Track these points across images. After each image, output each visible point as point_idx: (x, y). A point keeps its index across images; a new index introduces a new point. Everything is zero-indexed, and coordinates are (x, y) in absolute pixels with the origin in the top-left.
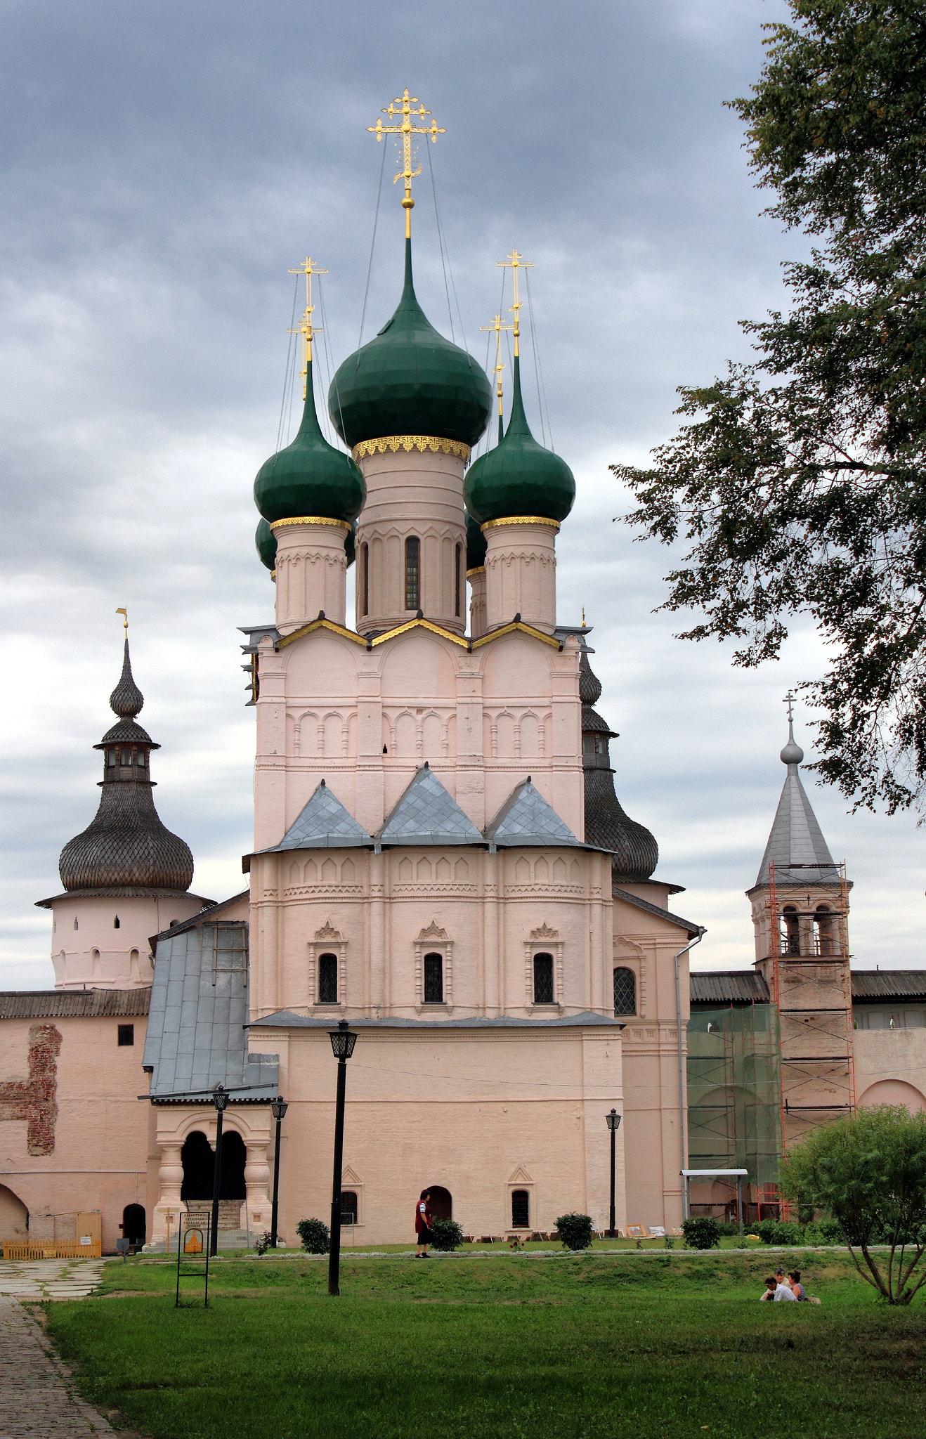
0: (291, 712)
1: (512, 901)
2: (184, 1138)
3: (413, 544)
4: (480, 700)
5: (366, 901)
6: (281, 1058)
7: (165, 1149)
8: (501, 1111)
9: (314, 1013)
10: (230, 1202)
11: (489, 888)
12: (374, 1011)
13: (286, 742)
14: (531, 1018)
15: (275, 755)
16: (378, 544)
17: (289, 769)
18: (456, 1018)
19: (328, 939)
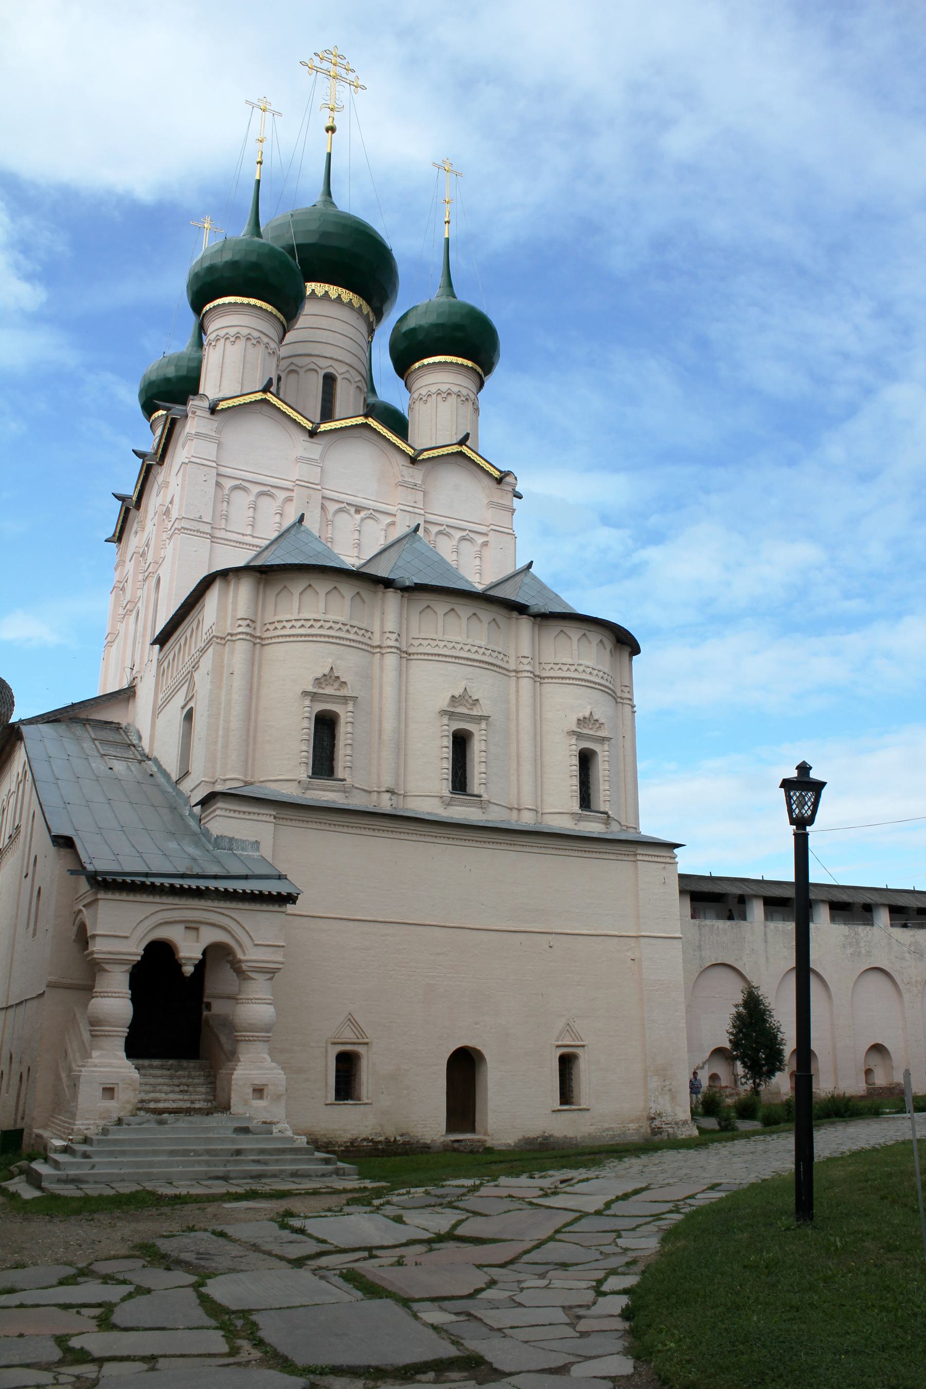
0: (222, 480)
1: (550, 681)
3: (329, 381)
4: (422, 512)
5: (378, 650)
7: (107, 967)
8: (547, 947)
9: (307, 789)
10: (185, 1063)
11: (525, 661)
12: (388, 795)
13: (214, 511)
14: (577, 828)
15: (200, 520)
16: (293, 377)
17: (213, 540)
18: (490, 818)
19: (329, 690)
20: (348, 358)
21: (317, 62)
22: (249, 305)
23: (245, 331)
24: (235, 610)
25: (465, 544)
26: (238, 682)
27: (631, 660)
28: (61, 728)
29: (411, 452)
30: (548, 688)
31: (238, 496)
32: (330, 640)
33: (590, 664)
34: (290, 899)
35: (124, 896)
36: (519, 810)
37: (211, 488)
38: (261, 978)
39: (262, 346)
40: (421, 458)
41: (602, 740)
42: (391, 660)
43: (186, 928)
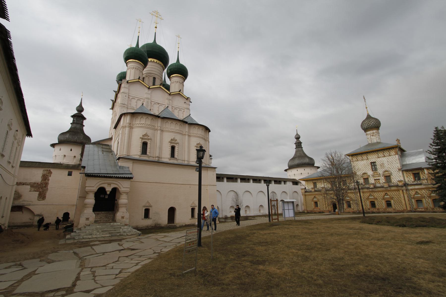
2: (97, 189)
3: (154, 78)
6: (130, 168)
7: (88, 193)
11: (187, 132)
12: (157, 158)
16: (147, 78)
18: (179, 162)
20: (158, 74)
21: (153, 13)
22: (136, 61)
23: (135, 67)
24: (126, 121)
25: (180, 111)
26: (126, 136)
27: (209, 133)
28: (95, 146)
29: (169, 93)
30: (191, 138)
31: (133, 100)
32: (146, 128)
33: (200, 133)
34: (131, 178)
35: (93, 178)
36: (185, 161)
37: (127, 98)
38: (124, 194)
39: (138, 70)
40: (171, 94)
41: (177, 143)
42: (159, 132)
43: (108, 184)
